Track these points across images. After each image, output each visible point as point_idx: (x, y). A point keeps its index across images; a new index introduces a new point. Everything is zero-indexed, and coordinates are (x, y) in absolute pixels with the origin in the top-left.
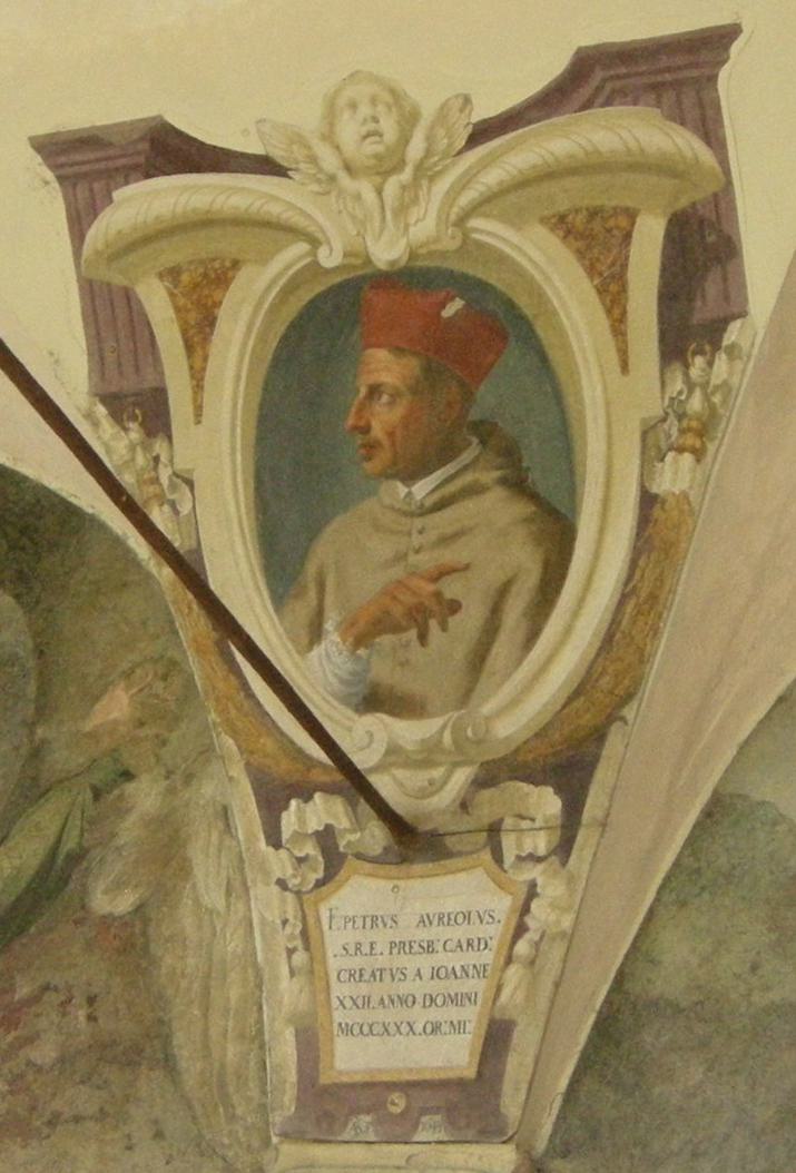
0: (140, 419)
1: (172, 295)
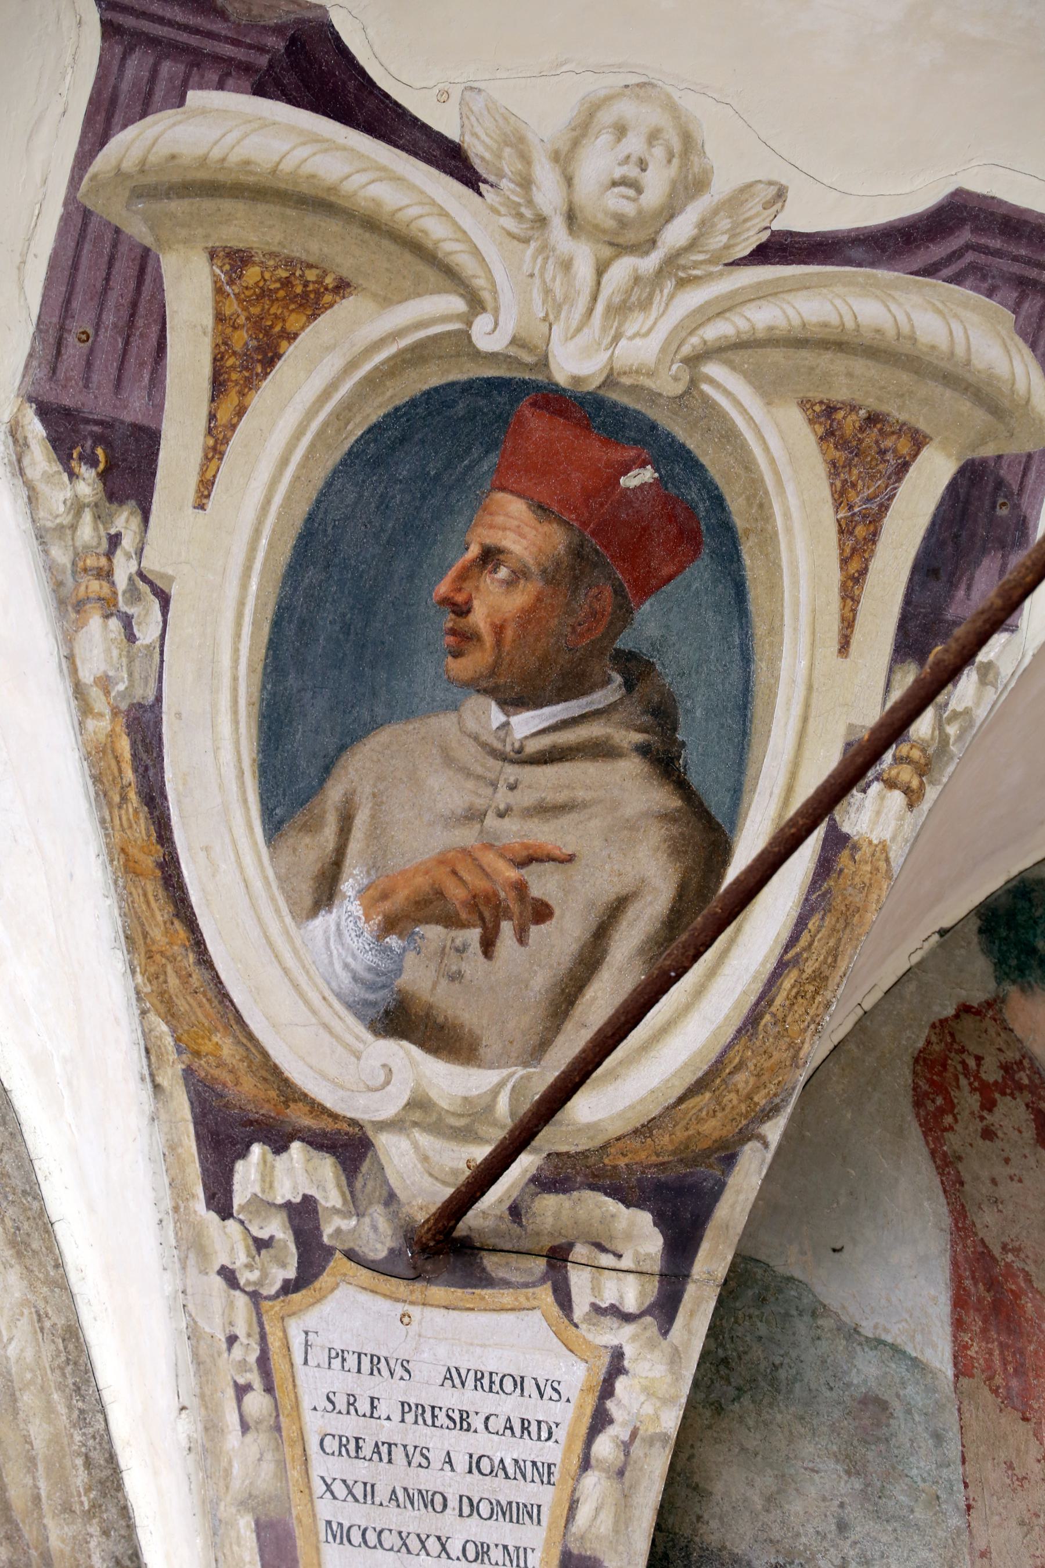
0: (102, 466)
1: (219, 291)
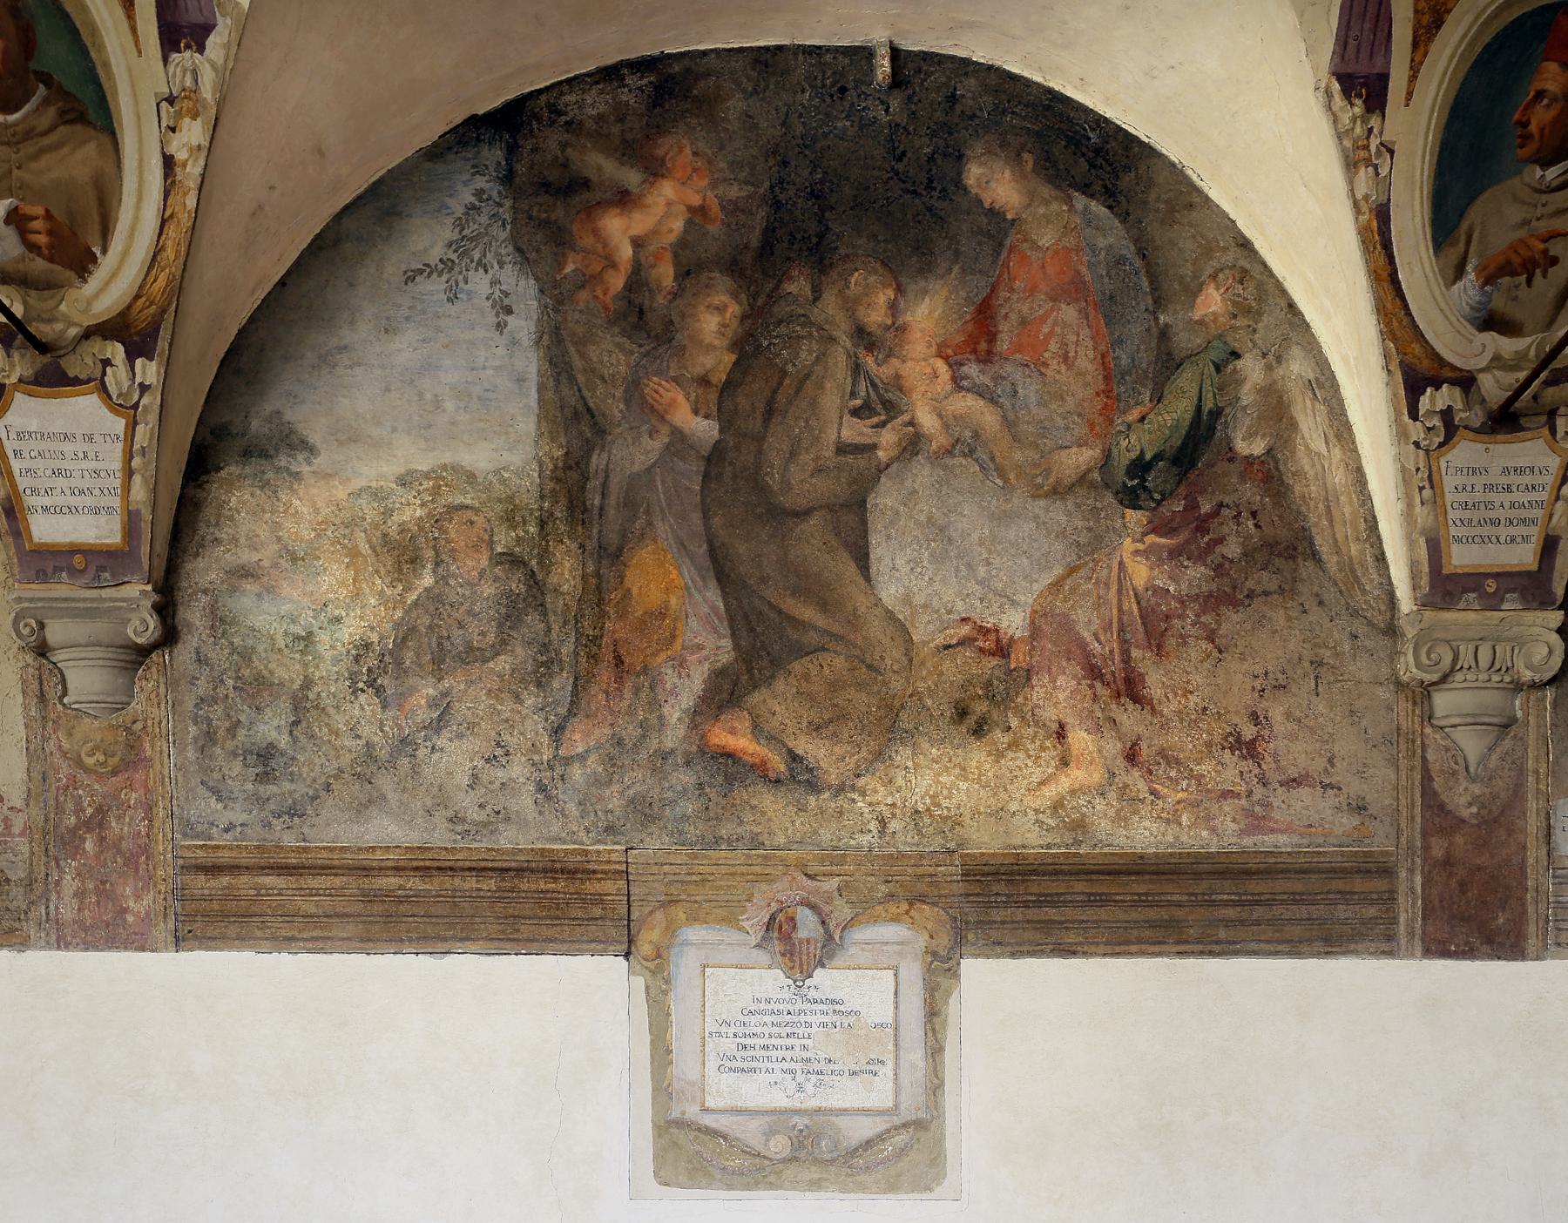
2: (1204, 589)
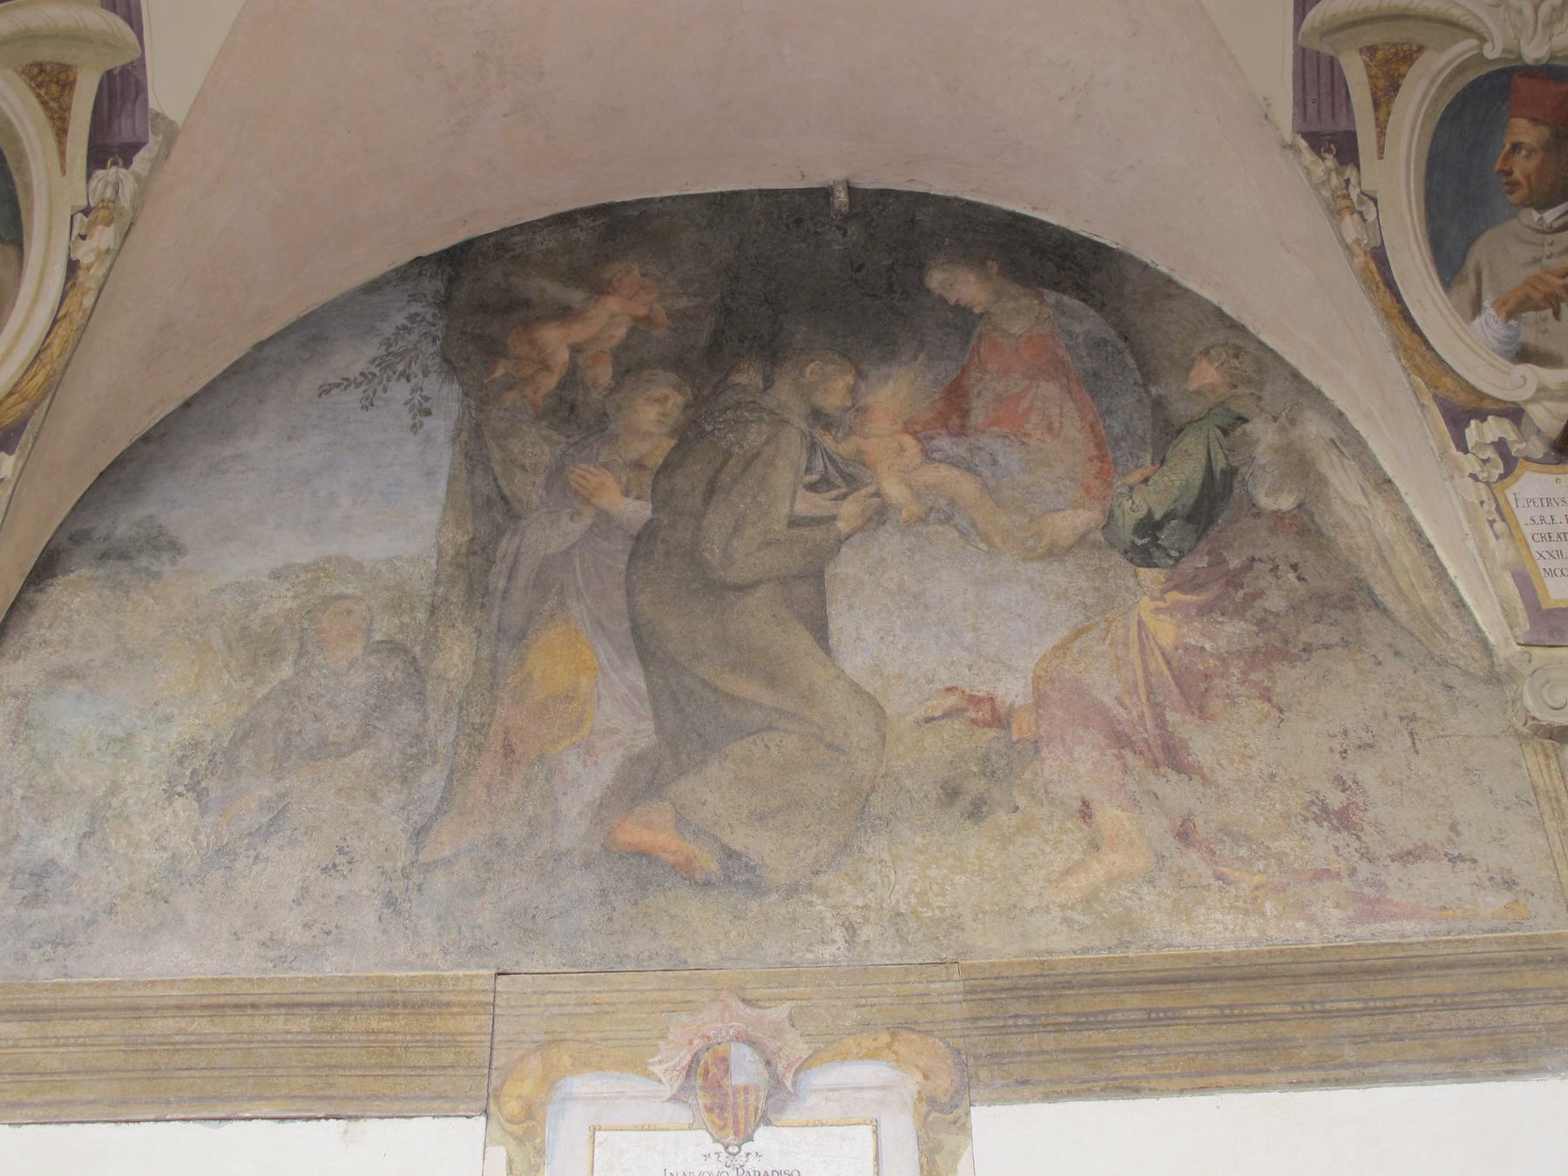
1: (1367, 66)
2: (1248, 644)
